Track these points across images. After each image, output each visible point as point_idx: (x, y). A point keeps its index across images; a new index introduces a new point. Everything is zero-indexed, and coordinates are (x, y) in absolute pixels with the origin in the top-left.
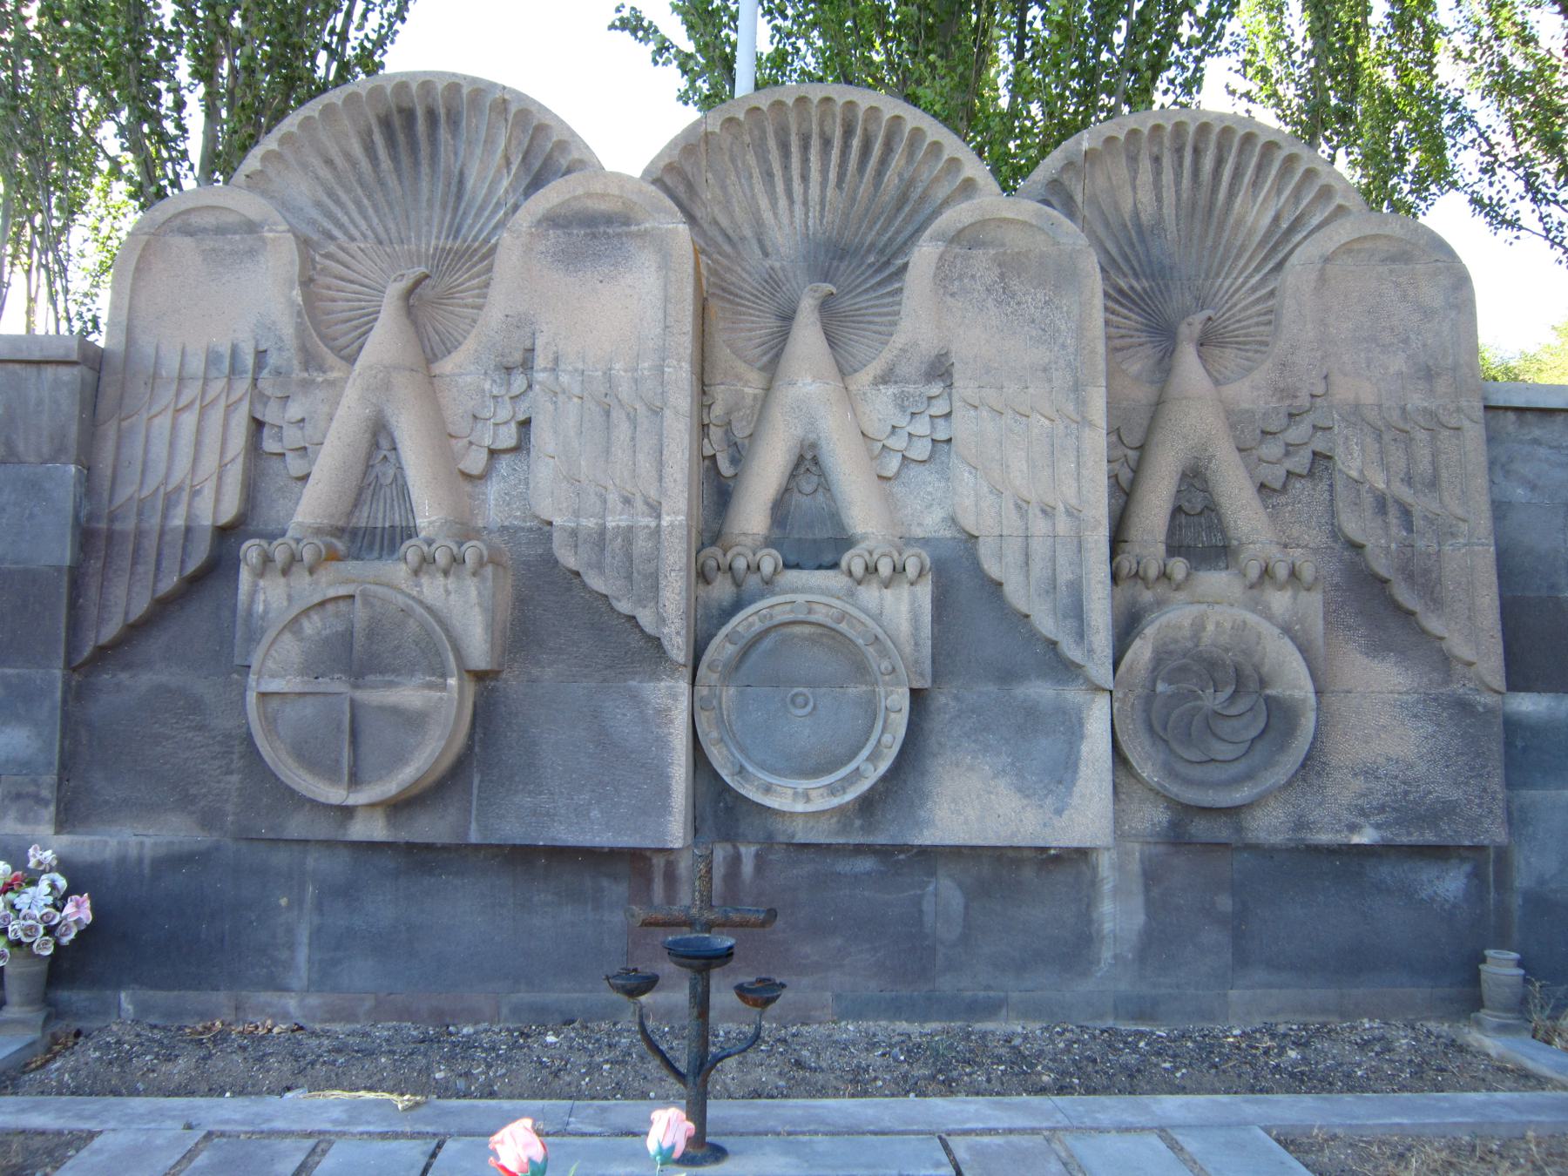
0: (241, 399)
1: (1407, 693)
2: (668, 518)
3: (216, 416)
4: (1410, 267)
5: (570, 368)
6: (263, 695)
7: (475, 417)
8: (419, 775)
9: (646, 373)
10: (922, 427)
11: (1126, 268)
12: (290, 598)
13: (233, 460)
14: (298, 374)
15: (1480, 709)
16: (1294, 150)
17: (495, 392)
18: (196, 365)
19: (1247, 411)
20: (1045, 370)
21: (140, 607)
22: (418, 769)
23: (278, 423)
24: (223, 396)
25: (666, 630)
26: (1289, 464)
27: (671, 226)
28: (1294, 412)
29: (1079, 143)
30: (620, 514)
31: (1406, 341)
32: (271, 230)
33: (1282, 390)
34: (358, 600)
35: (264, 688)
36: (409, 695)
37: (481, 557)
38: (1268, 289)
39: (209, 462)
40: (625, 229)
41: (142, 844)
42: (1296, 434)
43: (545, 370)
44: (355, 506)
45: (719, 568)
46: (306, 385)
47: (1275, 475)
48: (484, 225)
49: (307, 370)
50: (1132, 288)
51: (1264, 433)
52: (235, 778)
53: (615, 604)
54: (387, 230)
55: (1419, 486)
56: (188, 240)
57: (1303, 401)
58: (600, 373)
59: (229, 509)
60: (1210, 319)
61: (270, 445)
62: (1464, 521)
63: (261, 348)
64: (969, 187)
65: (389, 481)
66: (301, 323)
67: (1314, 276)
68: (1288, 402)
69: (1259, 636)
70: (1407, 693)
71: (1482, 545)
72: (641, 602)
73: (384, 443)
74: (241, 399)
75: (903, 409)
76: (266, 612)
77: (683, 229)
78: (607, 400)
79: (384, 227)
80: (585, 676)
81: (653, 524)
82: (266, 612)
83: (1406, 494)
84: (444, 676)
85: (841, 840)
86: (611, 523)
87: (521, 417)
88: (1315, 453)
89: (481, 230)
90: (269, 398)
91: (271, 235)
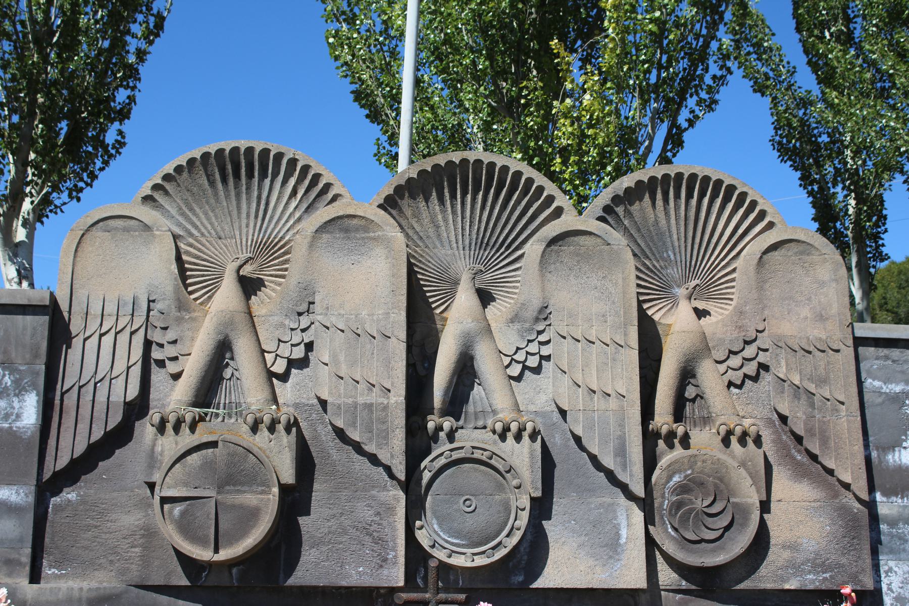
0: (139, 328)
1: (814, 501)
2: (395, 399)
3: (124, 338)
4: (811, 257)
5: (336, 313)
6: (164, 500)
7: (280, 340)
8: (256, 543)
9: (380, 317)
10: (534, 348)
11: (650, 255)
12: (177, 443)
13: (135, 364)
14: (174, 313)
15: (855, 511)
16: (744, 189)
17: (292, 326)
18: (111, 308)
19: (720, 339)
20: (603, 316)
21: (80, 449)
22: (255, 539)
23: (160, 342)
24: (129, 325)
25: (394, 462)
26: (745, 370)
27: (393, 234)
28: (748, 339)
29: (621, 184)
30: (367, 395)
31: (809, 299)
32: (158, 230)
33: (740, 327)
34: (220, 444)
35: (164, 494)
36: (250, 499)
37: (289, 420)
38: (732, 268)
39: (120, 366)
40: (367, 235)
41: (81, 589)
42: (750, 351)
43: (321, 314)
44: (208, 391)
45: (419, 429)
46: (179, 320)
47: (737, 377)
48: (281, 229)
49: (180, 312)
50: (654, 266)
51: (732, 352)
52: (137, 550)
53: (363, 446)
54: (223, 230)
55: (818, 383)
56: (108, 234)
57: (752, 334)
58: (353, 316)
59: (133, 392)
60: (697, 285)
61: (156, 354)
62: (843, 403)
63: (151, 299)
64: (559, 212)
65: (228, 377)
66: (178, 285)
67: (756, 261)
68: (744, 334)
69: (727, 467)
70: (814, 501)
71: (853, 416)
72: (379, 446)
73: (228, 355)
74: (139, 328)
75: (523, 337)
76: (162, 451)
77: (400, 236)
78: (359, 332)
79: (222, 228)
80: (346, 488)
81: (386, 402)
82: (162, 451)
83: (812, 388)
84: (268, 486)
85: (490, 586)
86: (361, 400)
87: (307, 340)
88: (759, 363)
89: (279, 232)
90: (156, 327)
91: (157, 233)
